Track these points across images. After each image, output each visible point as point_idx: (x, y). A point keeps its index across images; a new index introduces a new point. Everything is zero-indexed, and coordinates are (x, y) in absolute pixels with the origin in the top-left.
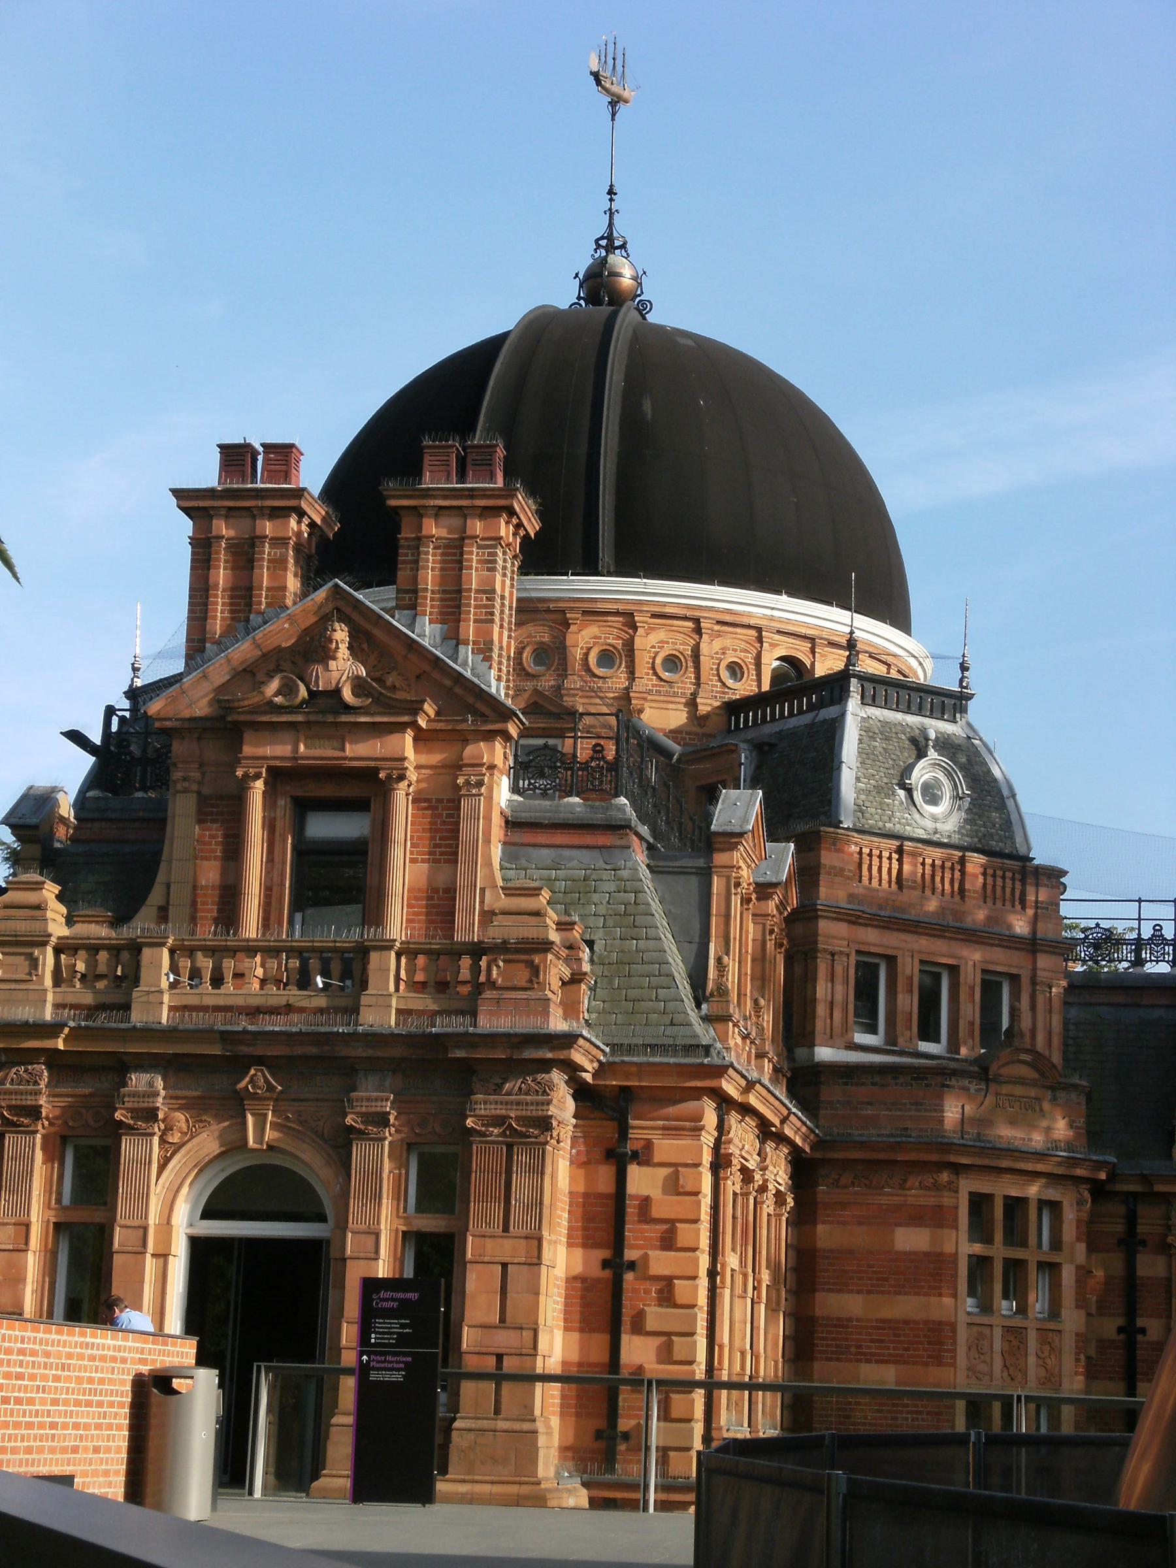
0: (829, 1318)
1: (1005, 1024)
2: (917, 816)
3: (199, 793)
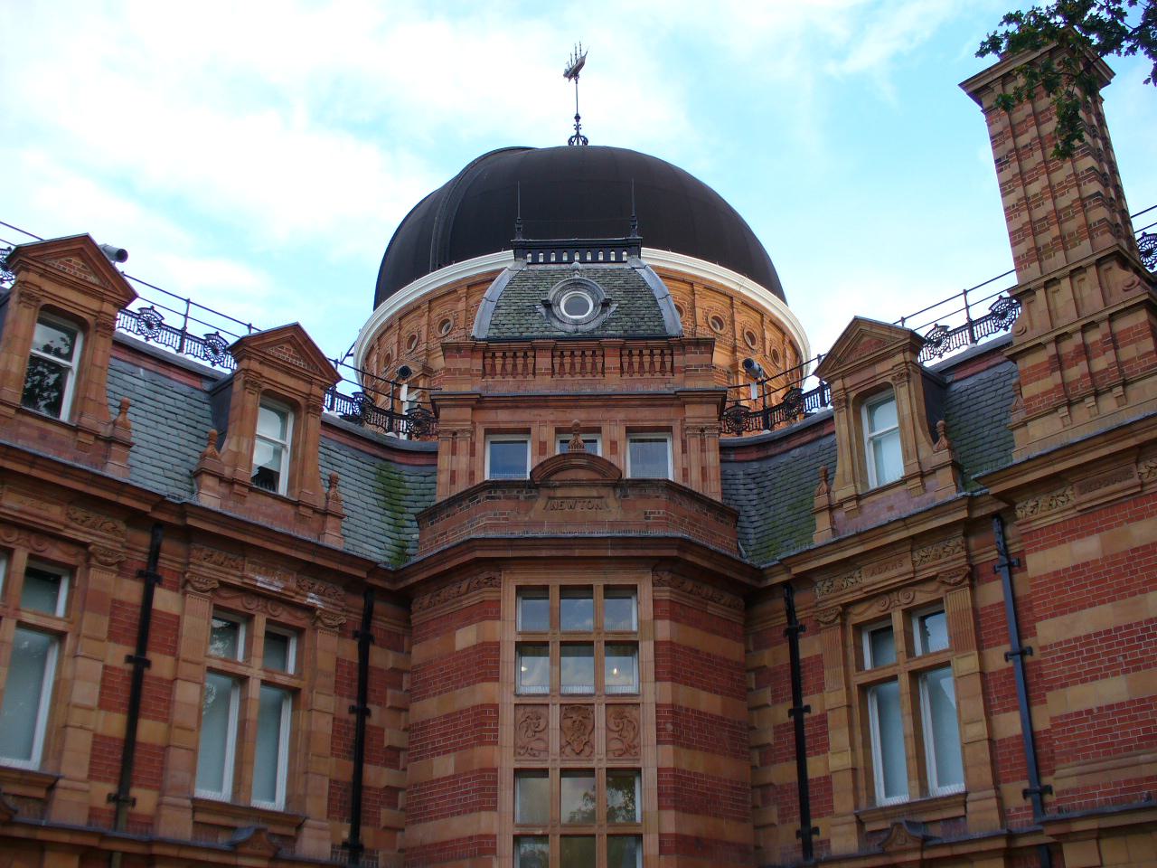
0: (417, 724)
2: (557, 324)
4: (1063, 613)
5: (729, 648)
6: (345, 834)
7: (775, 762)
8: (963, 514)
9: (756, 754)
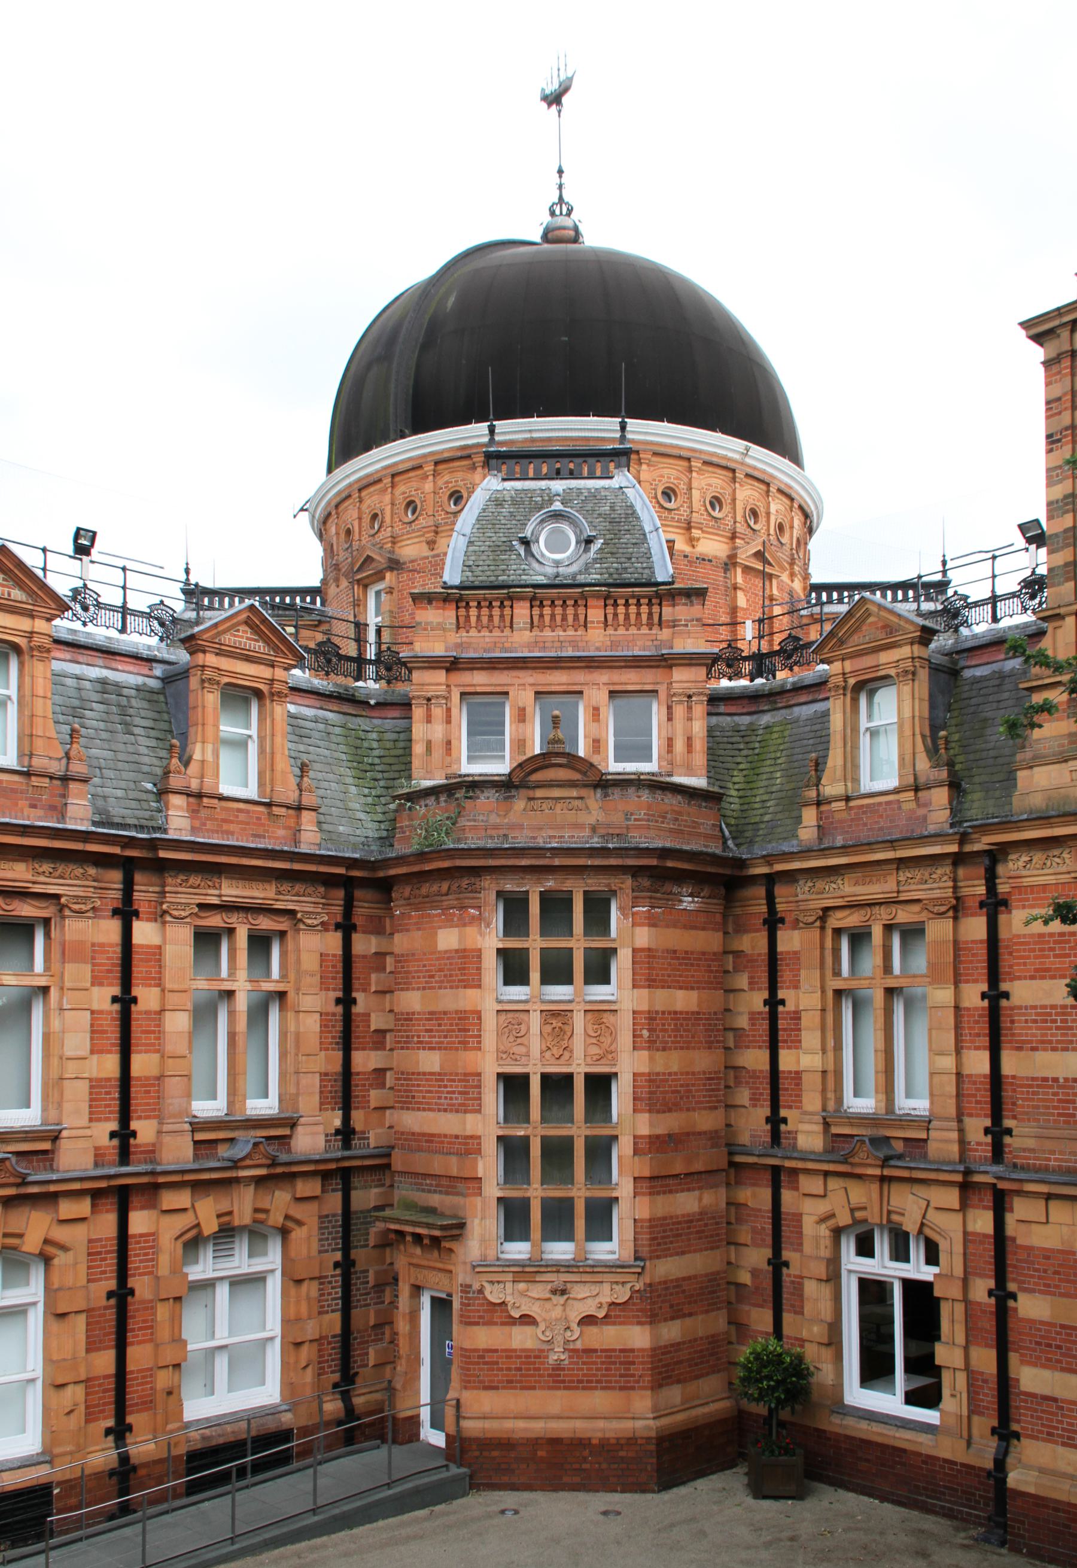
2: (535, 565)
4: (1043, 978)
5: (709, 941)
6: (338, 1123)
7: (748, 1047)
8: (954, 848)
9: (730, 1035)
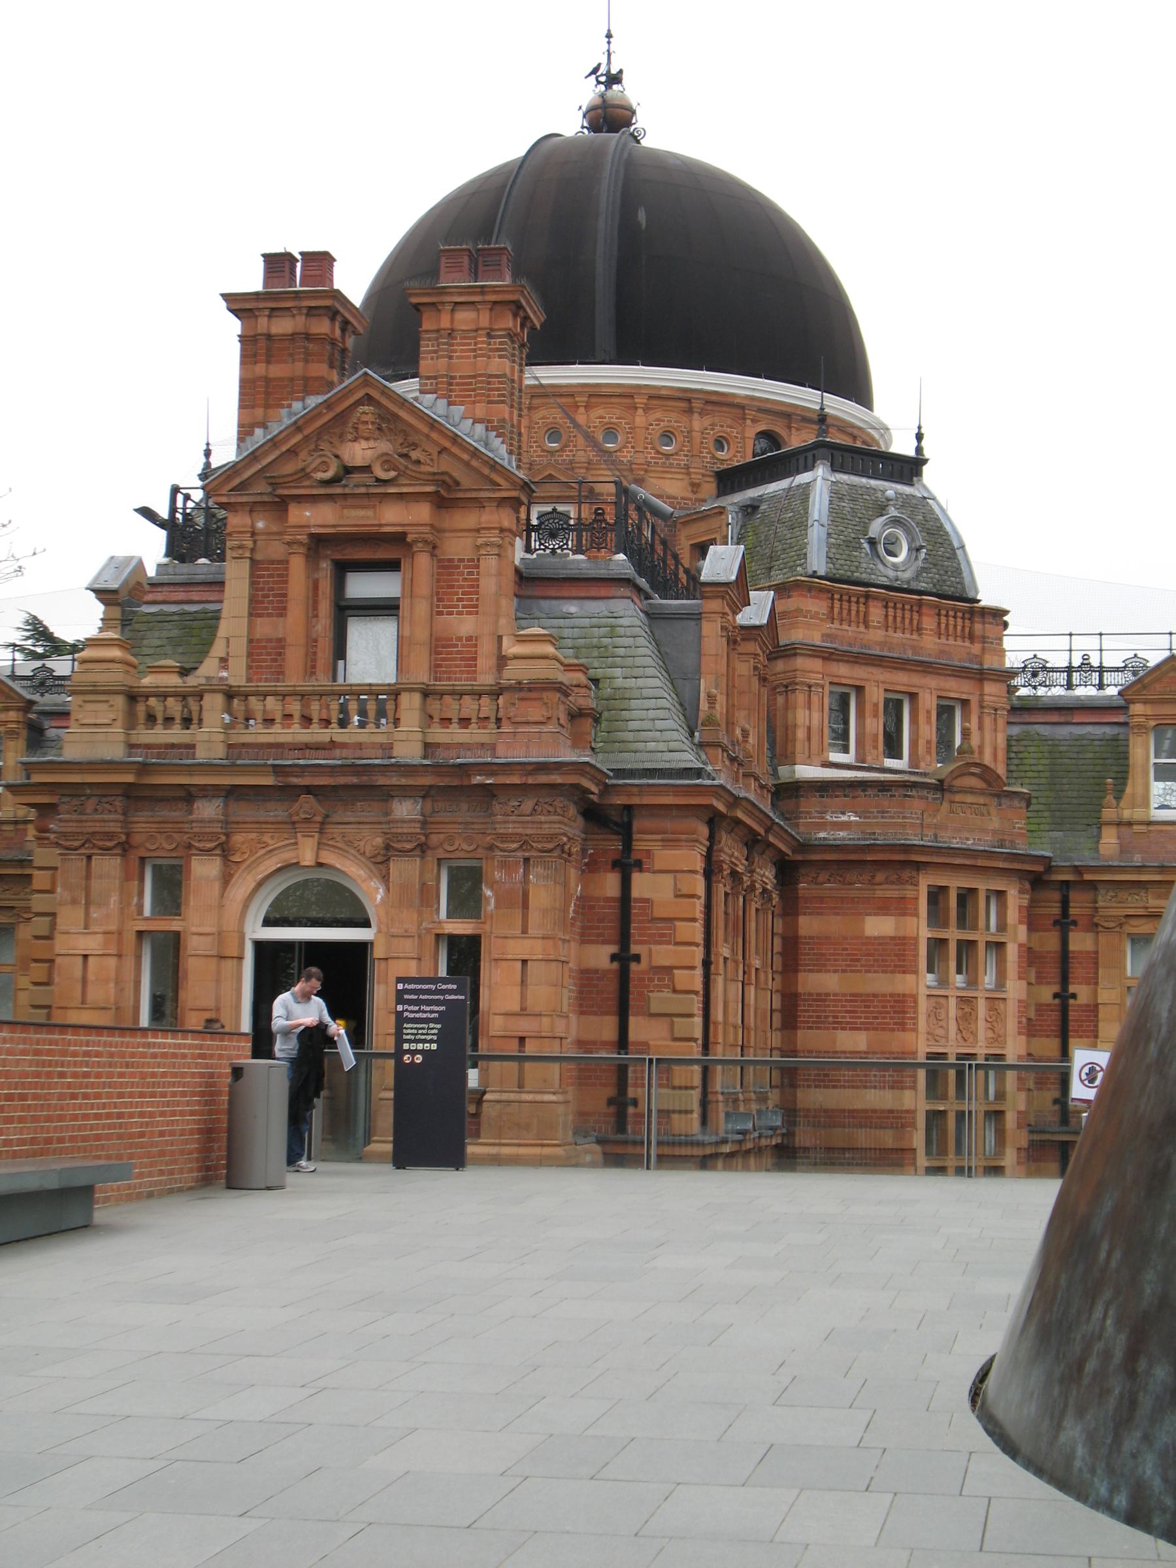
0: (810, 994)
1: (958, 742)
2: (880, 566)
3: (251, 559)
